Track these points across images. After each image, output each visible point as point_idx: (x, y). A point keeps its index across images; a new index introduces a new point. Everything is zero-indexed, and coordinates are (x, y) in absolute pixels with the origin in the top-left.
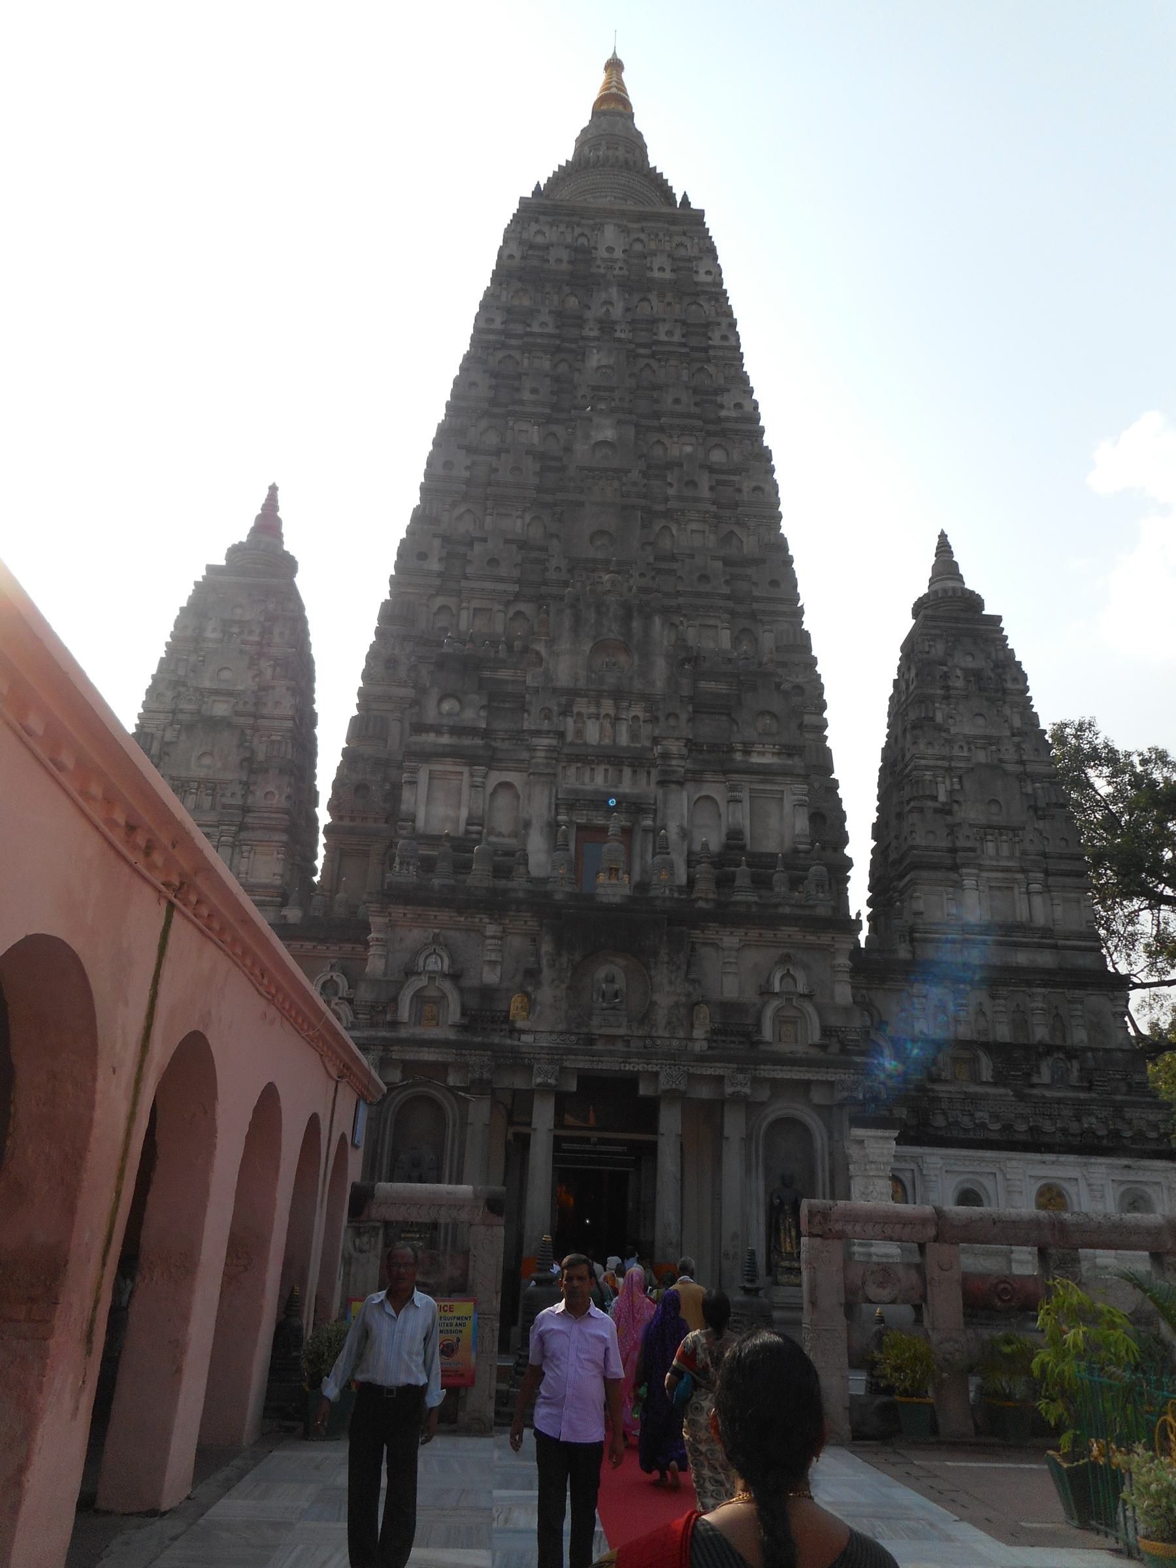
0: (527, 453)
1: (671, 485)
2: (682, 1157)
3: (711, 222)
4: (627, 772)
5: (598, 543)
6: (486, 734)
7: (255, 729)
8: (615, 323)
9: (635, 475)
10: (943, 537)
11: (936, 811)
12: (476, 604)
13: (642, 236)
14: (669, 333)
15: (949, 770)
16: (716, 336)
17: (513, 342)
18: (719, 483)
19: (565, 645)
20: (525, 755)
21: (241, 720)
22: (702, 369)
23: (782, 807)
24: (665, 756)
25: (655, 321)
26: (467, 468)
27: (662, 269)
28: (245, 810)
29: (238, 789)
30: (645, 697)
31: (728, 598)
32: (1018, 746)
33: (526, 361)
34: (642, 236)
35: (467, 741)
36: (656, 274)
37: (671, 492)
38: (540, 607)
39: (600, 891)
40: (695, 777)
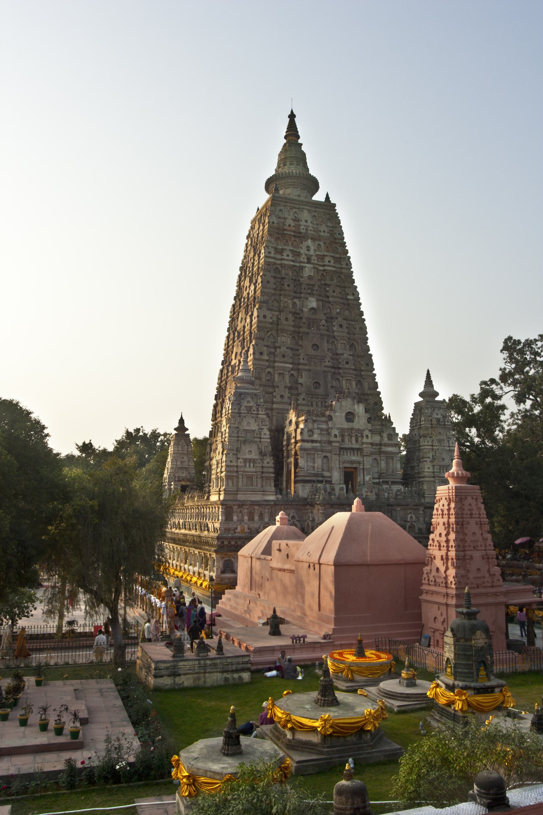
0: (290, 312)
1: (334, 326)
2: (406, 564)
3: (338, 209)
4: (356, 452)
5: (314, 348)
6: (320, 442)
7: (260, 442)
8: (312, 256)
9: (323, 322)
10: (428, 371)
11: (430, 462)
12: (281, 372)
13: (316, 214)
14: (329, 262)
15: (433, 449)
16: (344, 263)
17: (279, 262)
18: (349, 324)
19: (337, 414)
20: (330, 448)
21: (256, 440)
22: (340, 276)
23: (393, 461)
24: (365, 448)
25: (324, 256)
26: (271, 318)
27: (324, 231)
28: (262, 467)
29: (259, 461)
30: (359, 430)
31: (354, 370)
32: (448, 441)
33: (283, 271)
34: (316, 214)
35: (316, 445)
36: (322, 234)
37: (335, 329)
38: (298, 373)
39: (369, 497)
40: (372, 454)
